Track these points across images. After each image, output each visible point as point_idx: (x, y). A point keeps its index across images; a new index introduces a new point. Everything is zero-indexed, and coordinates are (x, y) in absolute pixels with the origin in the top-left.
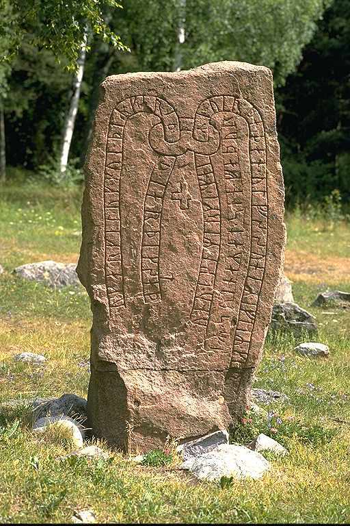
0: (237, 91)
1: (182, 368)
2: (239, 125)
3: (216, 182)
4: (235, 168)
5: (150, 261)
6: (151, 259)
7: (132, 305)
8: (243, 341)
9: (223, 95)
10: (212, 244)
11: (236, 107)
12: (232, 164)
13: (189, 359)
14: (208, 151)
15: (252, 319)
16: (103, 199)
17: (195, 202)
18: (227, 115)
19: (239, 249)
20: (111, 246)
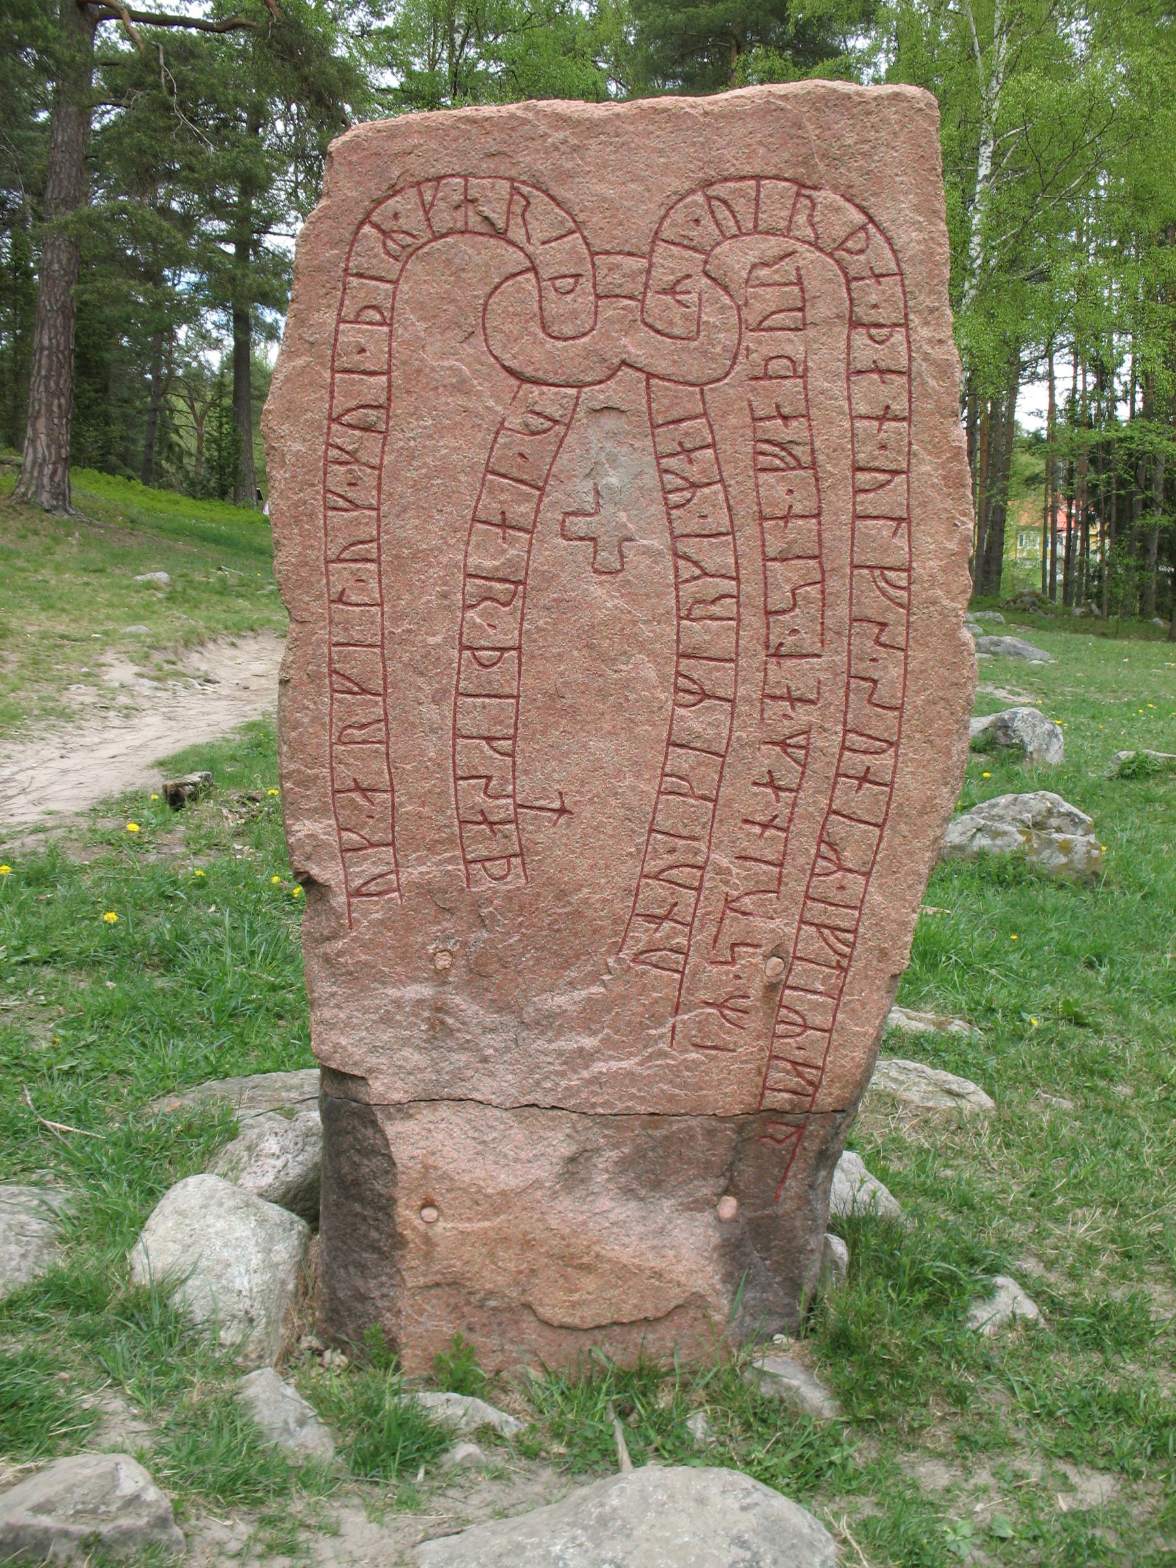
0: (805, 162)
1: (594, 1105)
2: (811, 285)
3: (721, 481)
4: (794, 430)
5: (486, 747)
6: (489, 739)
7: (426, 890)
8: (806, 1027)
9: (758, 178)
10: (705, 696)
11: (801, 219)
12: (785, 418)
13: (613, 1076)
14: (694, 368)
15: (843, 955)
16: (321, 534)
17: (647, 551)
18: (772, 246)
19: (803, 715)
20: (351, 692)
